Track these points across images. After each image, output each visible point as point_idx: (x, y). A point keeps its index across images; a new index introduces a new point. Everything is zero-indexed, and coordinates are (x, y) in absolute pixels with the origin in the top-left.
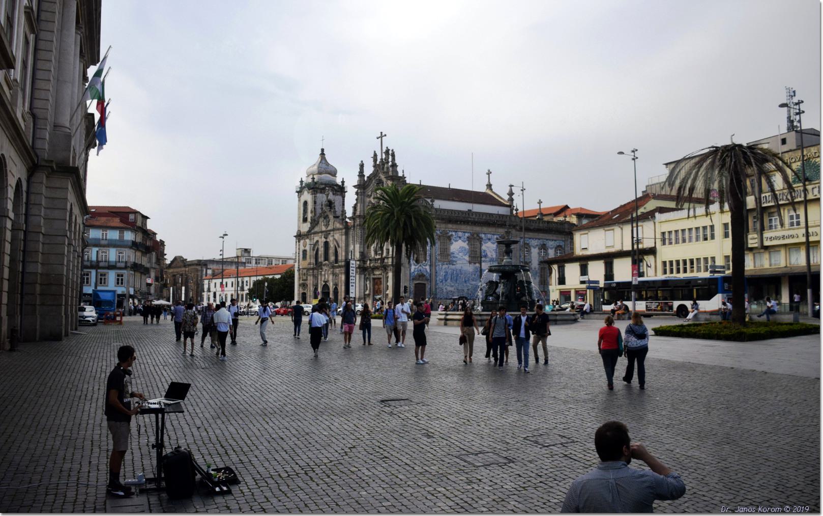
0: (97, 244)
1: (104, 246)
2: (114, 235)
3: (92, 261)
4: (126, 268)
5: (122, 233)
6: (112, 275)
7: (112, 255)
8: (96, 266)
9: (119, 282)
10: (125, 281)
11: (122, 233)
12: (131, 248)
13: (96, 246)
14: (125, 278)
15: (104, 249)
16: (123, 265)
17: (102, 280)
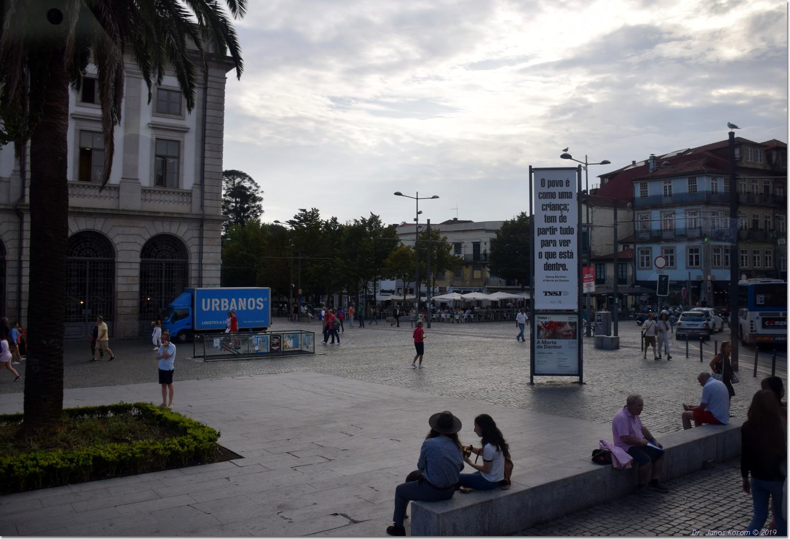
0: (656, 203)
2: (680, 186)
3: (650, 232)
4: (702, 237)
5: (692, 181)
7: (681, 220)
8: (657, 238)
9: (694, 260)
10: (702, 260)
11: (692, 181)
13: (655, 207)
14: (701, 254)
15: (669, 210)
17: (671, 262)
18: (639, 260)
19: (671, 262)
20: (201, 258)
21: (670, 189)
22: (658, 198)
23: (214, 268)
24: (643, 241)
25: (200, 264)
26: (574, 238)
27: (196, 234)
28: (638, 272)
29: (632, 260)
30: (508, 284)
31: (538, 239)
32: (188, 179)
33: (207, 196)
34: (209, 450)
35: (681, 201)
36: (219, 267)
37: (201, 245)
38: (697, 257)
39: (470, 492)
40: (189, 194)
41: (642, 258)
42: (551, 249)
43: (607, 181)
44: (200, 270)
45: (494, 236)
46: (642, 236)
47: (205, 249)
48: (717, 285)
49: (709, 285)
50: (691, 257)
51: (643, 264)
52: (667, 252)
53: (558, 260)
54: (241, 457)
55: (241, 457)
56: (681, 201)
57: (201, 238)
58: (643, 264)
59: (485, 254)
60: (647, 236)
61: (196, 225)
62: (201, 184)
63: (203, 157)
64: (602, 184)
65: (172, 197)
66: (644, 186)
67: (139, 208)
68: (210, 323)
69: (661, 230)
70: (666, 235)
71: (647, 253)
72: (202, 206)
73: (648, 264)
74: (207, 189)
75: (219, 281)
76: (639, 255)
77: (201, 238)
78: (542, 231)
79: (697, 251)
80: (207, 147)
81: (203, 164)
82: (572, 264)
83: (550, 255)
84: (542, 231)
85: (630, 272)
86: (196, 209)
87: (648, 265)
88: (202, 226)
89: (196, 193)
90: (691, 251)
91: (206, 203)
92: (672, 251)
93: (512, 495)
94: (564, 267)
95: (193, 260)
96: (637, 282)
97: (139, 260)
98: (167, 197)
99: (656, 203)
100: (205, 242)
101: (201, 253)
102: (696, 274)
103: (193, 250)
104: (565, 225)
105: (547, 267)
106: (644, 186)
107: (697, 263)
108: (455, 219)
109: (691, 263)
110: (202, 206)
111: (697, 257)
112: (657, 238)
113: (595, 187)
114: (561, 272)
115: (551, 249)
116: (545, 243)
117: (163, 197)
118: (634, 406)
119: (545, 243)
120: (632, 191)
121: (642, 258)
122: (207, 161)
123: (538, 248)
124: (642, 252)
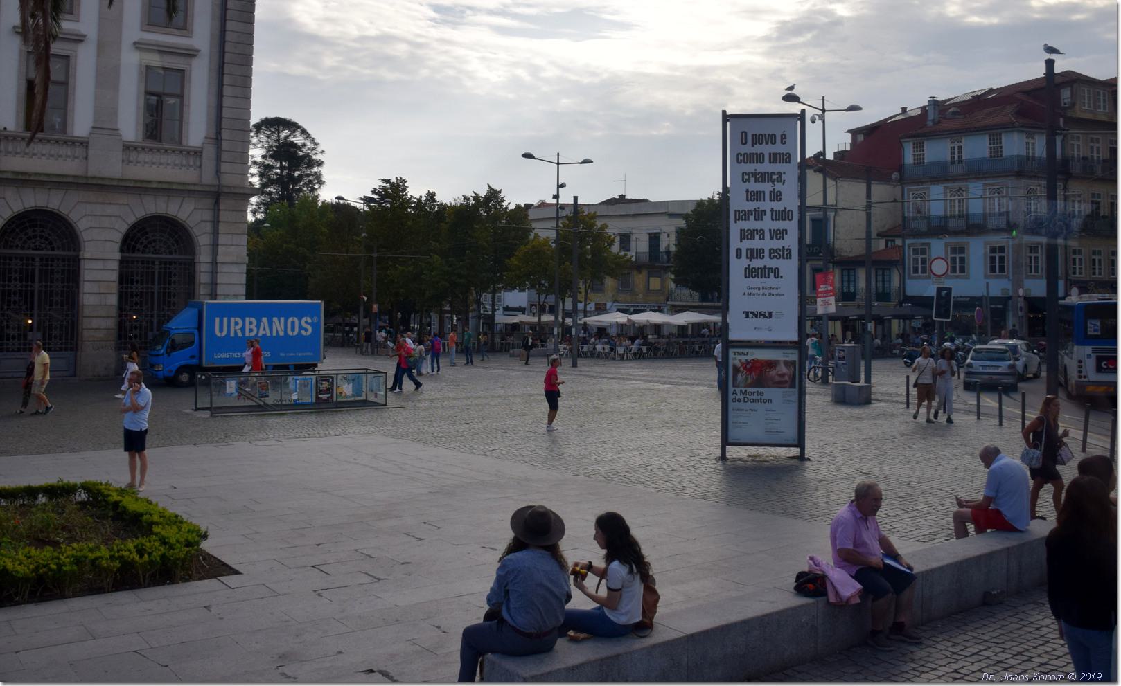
0: (939, 174)
1: (955, 179)
2: (976, 148)
4: (1010, 227)
5: (995, 140)
6: (977, 249)
7: (977, 199)
8: (939, 228)
9: (997, 263)
10: (1009, 264)
11: (995, 140)
12: (1020, 174)
13: (935, 180)
14: (1009, 255)
16: (1002, 222)
17: (959, 266)
18: (909, 263)
19: (959, 266)
20: (215, 253)
21: (960, 152)
22: (942, 165)
23: (235, 269)
24: (917, 234)
25: (214, 263)
26: (792, 226)
27: (208, 215)
28: (908, 282)
29: (899, 263)
30: (704, 299)
31: (735, 229)
32: (197, 130)
33: (225, 156)
34: (184, 561)
35: (976, 171)
36: (244, 268)
37: (215, 233)
38: (1002, 259)
39: (583, 639)
40: (197, 153)
41: (916, 260)
42: (756, 244)
43: (861, 138)
44: (214, 273)
45: (681, 223)
46: (914, 225)
47: (222, 239)
48: (1033, 304)
49: (1021, 303)
50: (993, 259)
51: (916, 271)
52: (954, 250)
53: (767, 262)
54: (237, 573)
55: (237, 573)
56: (976, 171)
57: (216, 222)
58: (916, 271)
59: (668, 252)
60: (923, 226)
61: (209, 202)
62: (217, 138)
63: (220, 95)
64: (854, 143)
65: (171, 158)
66: (919, 147)
67: (118, 176)
68: (227, 355)
69: (945, 217)
70: (953, 224)
71: (923, 252)
72: (218, 172)
73: (924, 268)
74: (225, 145)
75: (243, 290)
76: (909, 256)
77: (216, 222)
78: (743, 215)
79: (1002, 249)
80: (226, 79)
81: (220, 107)
82: (789, 268)
83: (755, 254)
84: (743, 215)
85: (896, 281)
86: (208, 177)
87: (924, 271)
88: (217, 203)
89: (209, 152)
90: (993, 250)
91: (225, 167)
92: (962, 250)
93: (654, 646)
94: (776, 272)
95: (203, 257)
96: (907, 299)
97: (118, 256)
98: (163, 158)
99: (939, 174)
100: (222, 228)
101: (215, 245)
102: (998, 287)
103: (203, 240)
104: (778, 206)
105: (750, 273)
106: (919, 147)
107: (1002, 269)
108: (622, 197)
109: (993, 269)
110: (218, 172)
111: (1002, 259)
112: (939, 228)
113: (842, 148)
114: (771, 281)
115: (756, 244)
116: (747, 235)
117: (157, 157)
118: (867, 501)
119: (747, 235)
120: (901, 155)
121: (916, 260)
122: (227, 102)
123: (735, 242)
124: (916, 251)
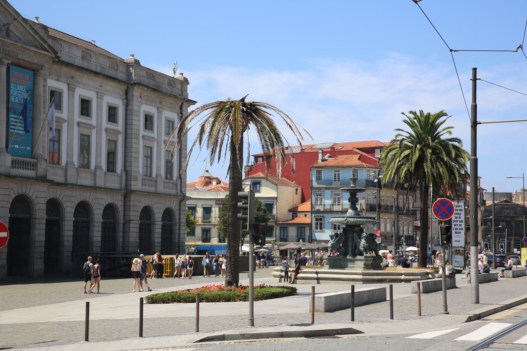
21: (339, 176)
26: (463, 224)
31: (453, 224)
37: (180, 214)
41: (317, 224)
42: (456, 227)
53: (458, 231)
58: (317, 228)
71: (321, 220)
77: (180, 210)
78: (454, 221)
82: (463, 232)
84: (454, 221)
94: (460, 233)
97: (102, 220)
103: (177, 217)
104: (460, 220)
105: (456, 233)
114: (459, 234)
115: (456, 227)
116: (455, 225)
119: (455, 225)
123: (453, 227)
124: (317, 220)
